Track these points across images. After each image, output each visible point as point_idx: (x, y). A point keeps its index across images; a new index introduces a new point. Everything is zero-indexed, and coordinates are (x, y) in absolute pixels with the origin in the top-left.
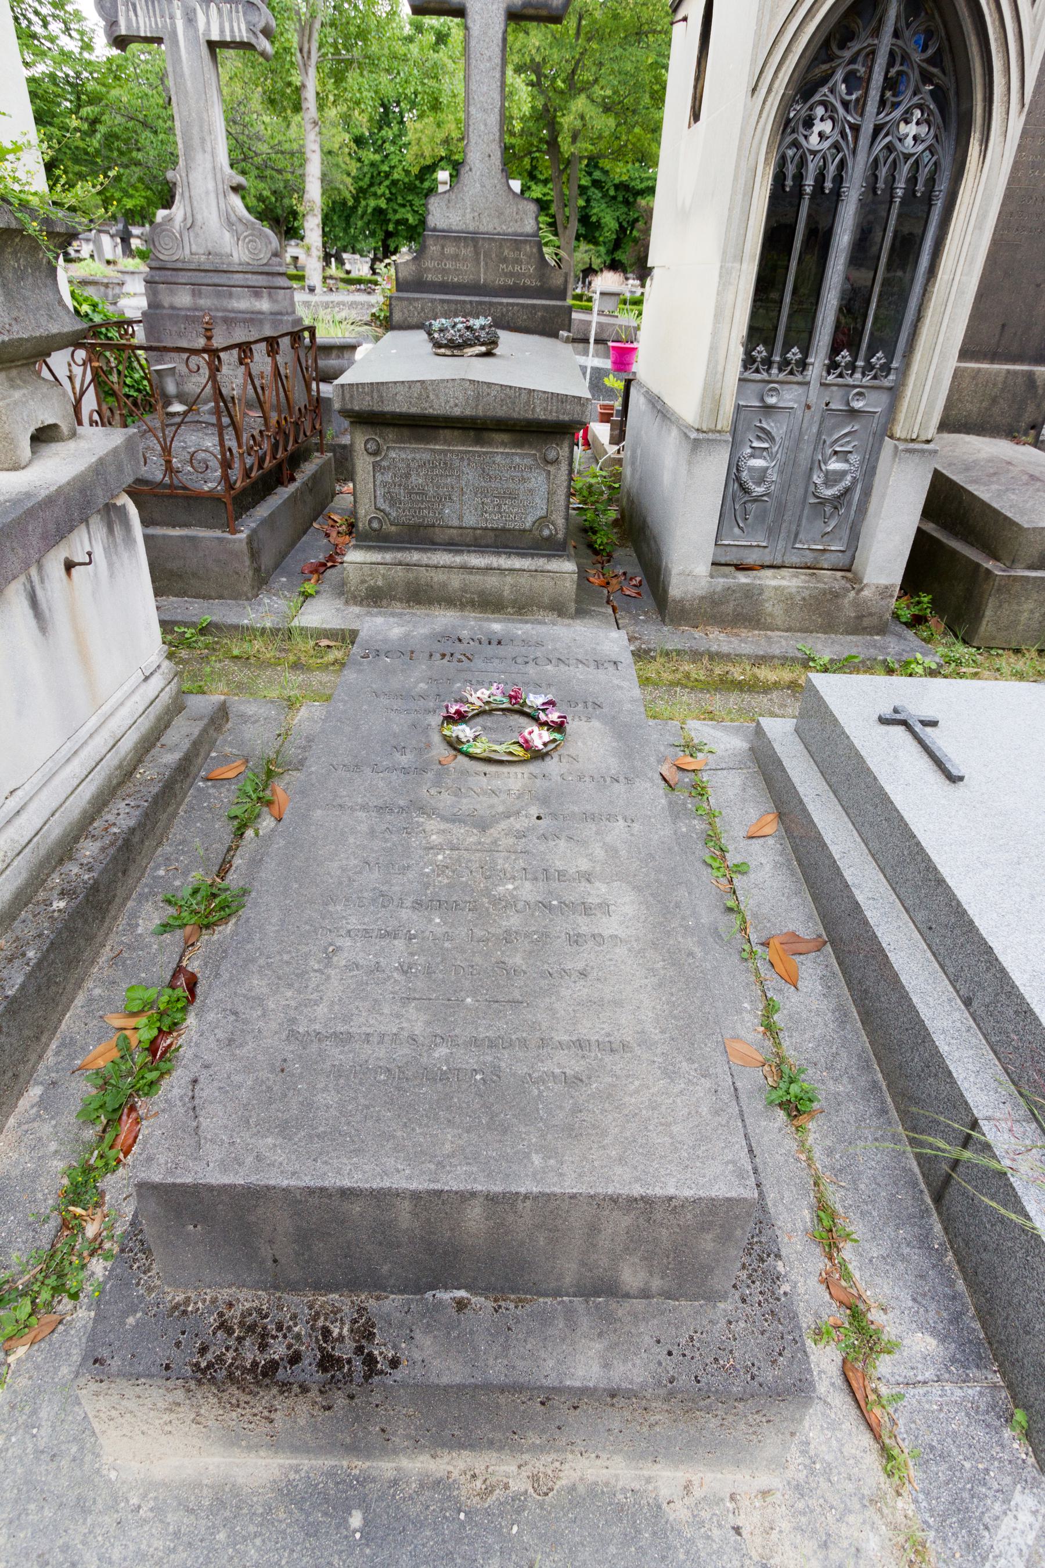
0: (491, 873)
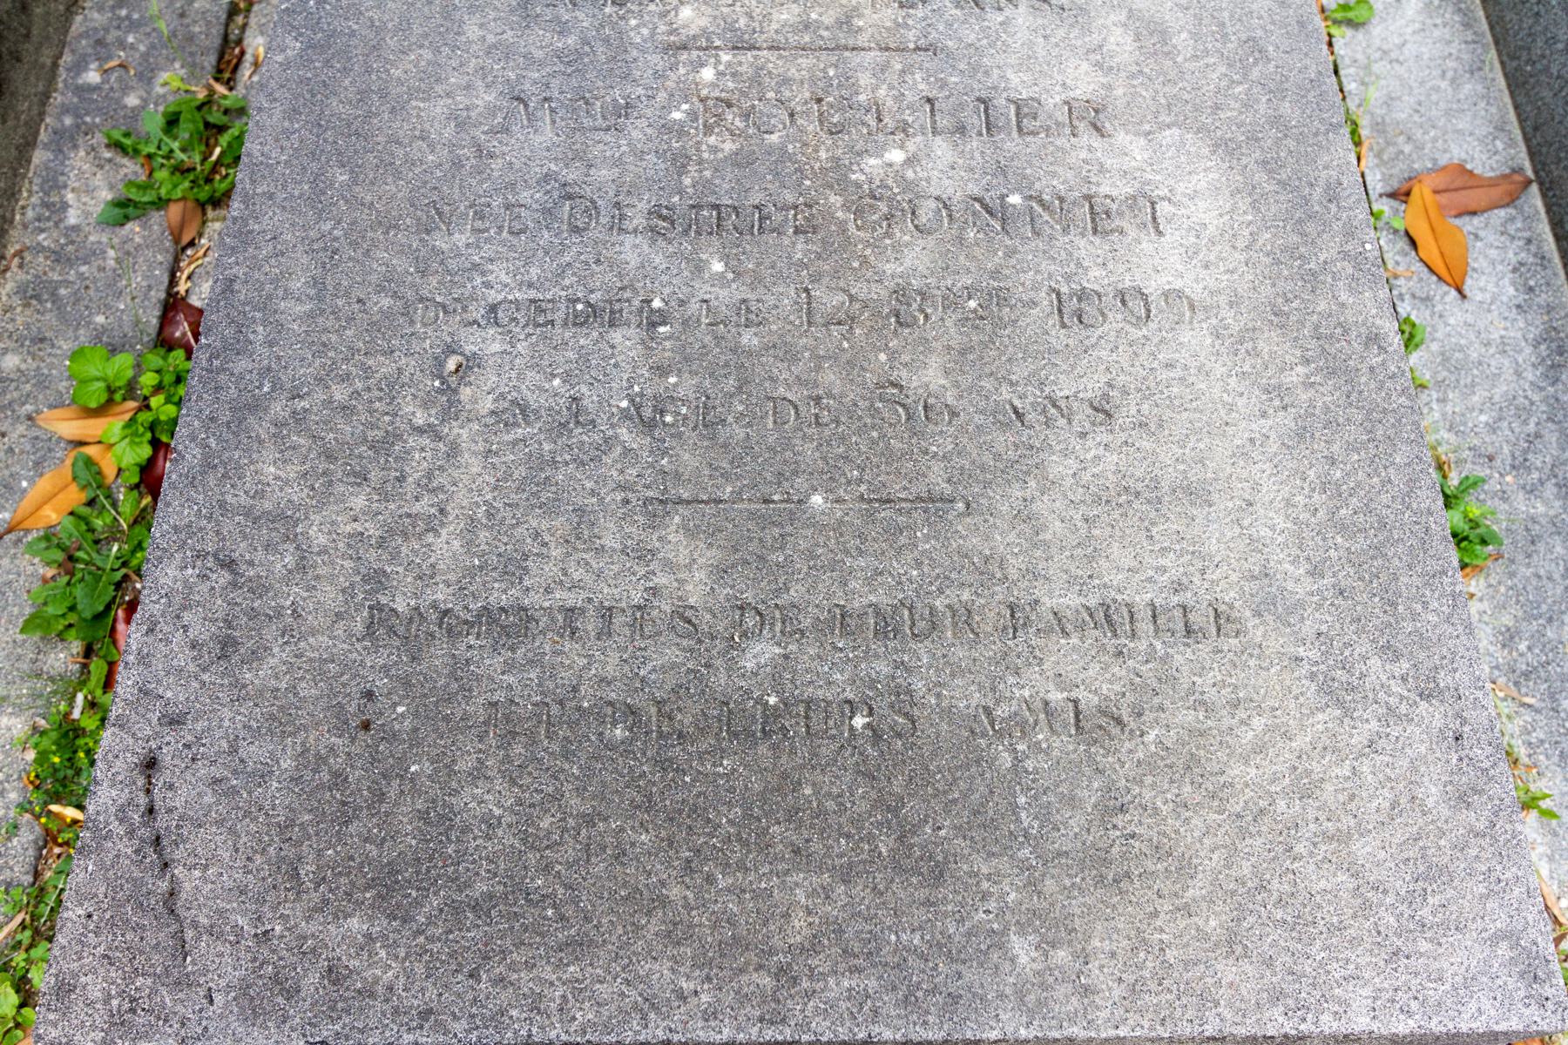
0: (839, 113)
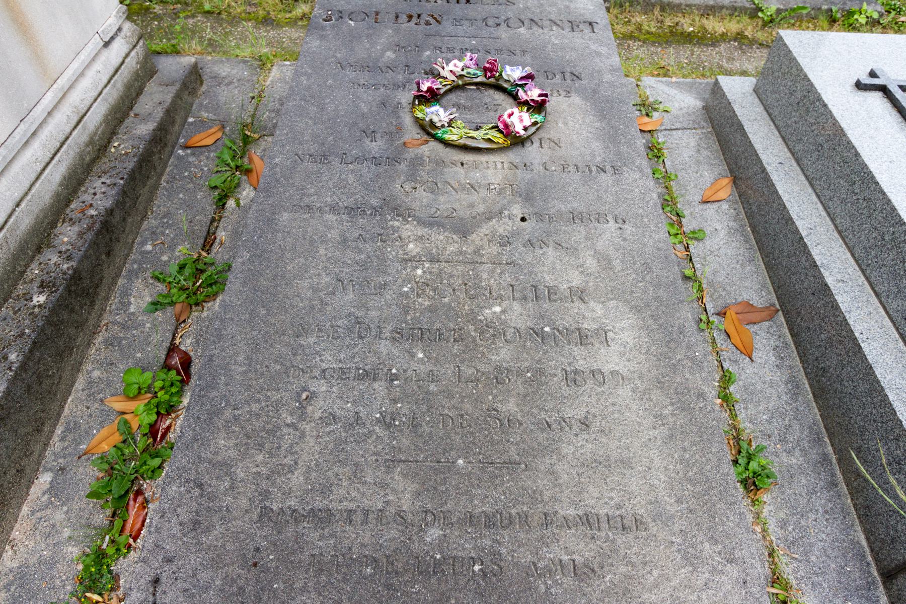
0: (475, 291)
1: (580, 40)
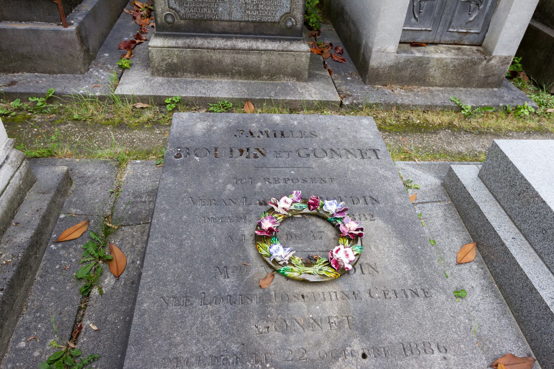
1: (369, 166)
